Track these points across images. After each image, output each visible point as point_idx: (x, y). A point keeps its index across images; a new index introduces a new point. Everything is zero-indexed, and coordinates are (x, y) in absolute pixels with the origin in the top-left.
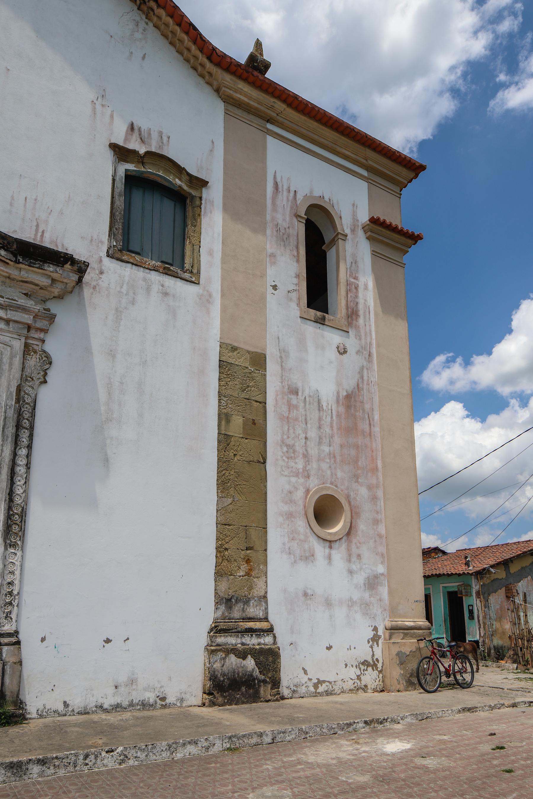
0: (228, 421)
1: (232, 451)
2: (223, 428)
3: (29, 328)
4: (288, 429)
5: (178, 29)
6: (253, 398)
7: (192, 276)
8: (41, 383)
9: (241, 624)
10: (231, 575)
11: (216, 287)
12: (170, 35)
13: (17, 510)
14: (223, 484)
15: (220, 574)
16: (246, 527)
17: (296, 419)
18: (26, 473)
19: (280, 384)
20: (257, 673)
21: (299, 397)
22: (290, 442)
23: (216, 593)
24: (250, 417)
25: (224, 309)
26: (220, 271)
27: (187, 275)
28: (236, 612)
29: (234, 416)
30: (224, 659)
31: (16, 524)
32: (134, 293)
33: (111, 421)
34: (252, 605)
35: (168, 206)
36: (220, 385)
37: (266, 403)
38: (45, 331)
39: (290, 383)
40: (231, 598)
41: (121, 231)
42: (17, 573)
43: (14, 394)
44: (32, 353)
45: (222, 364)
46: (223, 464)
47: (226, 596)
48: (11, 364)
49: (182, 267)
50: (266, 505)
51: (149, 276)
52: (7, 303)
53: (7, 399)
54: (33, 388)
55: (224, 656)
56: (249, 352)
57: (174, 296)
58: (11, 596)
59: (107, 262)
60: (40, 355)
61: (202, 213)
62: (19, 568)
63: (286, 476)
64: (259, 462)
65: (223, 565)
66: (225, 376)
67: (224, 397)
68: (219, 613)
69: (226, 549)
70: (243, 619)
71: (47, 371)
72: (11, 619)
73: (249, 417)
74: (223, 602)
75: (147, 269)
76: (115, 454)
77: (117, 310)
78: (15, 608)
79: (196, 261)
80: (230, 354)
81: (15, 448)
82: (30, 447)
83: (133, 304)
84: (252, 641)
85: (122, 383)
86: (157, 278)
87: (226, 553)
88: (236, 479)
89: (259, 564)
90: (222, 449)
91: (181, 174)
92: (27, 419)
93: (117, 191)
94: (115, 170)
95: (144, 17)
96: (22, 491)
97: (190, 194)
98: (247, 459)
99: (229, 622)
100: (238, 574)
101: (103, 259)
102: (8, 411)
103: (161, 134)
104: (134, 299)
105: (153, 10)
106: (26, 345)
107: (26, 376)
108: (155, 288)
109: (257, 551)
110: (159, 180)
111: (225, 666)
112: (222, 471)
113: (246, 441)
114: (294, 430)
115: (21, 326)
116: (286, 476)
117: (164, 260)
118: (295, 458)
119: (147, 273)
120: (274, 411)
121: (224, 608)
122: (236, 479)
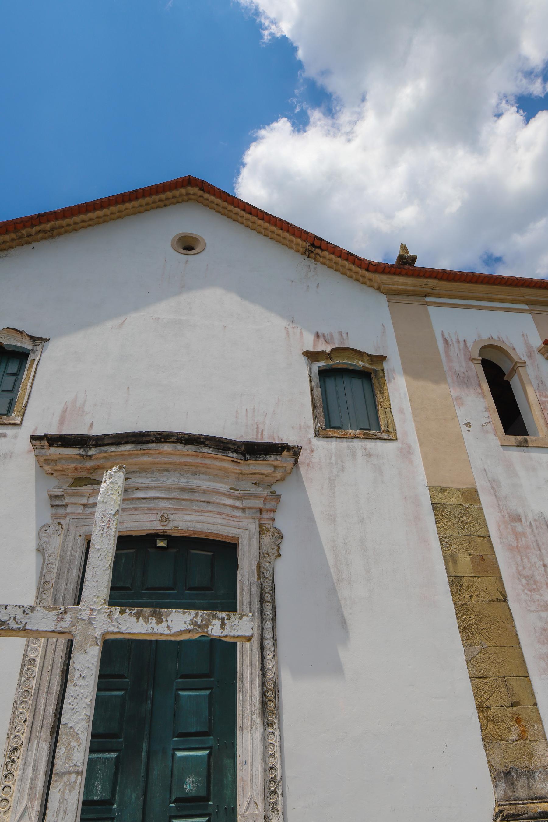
0: (455, 562)
1: (467, 593)
2: (451, 570)
3: (261, 511)
4: (521, 559)
5: (339, 259)
6: (475, 534)
7: (390, 435)
8: (276, 557)
9: (531, 806)
10: (502, 740)
11: (413, 438)
12: (334, 265)
13: (270, 686)
14: (466, 631)
16: (504, 677)
17: (527, 547)
18: (274, 645)
19: (499, 514)
21: (523, 523)
22: (527, 572)
23: (490, 766)
24: (477, 554)
25: (425, 457)
26: (413, 424)
27: (384, 435)
28: (520, 790)
29: (459, 556)
31: (270, 700)
32: (342, 461)
33: (342, 581)
34: (538, 778)
35: (357, 384)
36: (438, 528)
37: (489, 536)
38: (273, 511)
39: (509, 510)
40: (510, 771)
41: (322, 414)
42: (278, 755)
43: (256, 571)
44: (266, 532)
45: (435, 506)
46: (462, 610)
47: (503, 769)
48: (250, 545)
49: (379, 429)
50: (521, 649)
51: (352, 444)
52: (241, 494)
53: (250, 577)
54: (270, 563)
56: (458, 490)
57: (377, 455)
58: (275, 783)
59: (315, 441)
60: (273, 532)
61: (387, 381)
62: (279, 749)
63: (534, 611)
64: (499, 600)
65: (490, 728)
66: (441, 517)
67: (446, 538)
68: (501, 792)
69: (489, 708)
70: (532, 799)
71: (280, 546)
72: (278, 811)
73: (476, 553)
74: (502, 777)
75: (350, 438)
76: (351, 614)
77: (330, 479)
78: (280, 797)
79: (390, 422)
80: (441, 495)
81: (262, 623)
82: (274, 619)
83: (343, 471)
85: (345, 544)
86: (359, 443)
87: (490, 712)
88: (479, 623)
89: (532, 724)
90: (456, 593)
91: (362, 357)
92: (269, 593)
93: (314, 385)
94: (310, 370)
95: (313, 261)
96: (272, 665)
97: (373, 370)
98: (486, 599)
99: (515, 804)
101: (312, 440)
102: (252, 588)
103: (340, 334)
104: (343, 466)
105: (318, 254)
106: (261, 526)
107: (263, 553)
108: (359, 453)
109: (525, 706)
110: (345, 367)
112: (462, 616)
113: (479, 579)
114: (528, 558)
115: (254, 511)
116: (534, 611)
117: (362, 427)
118: (539, 590)
119: (350, 442)
120: (501, 543)
121: (504, 785)
122: (479, 623)
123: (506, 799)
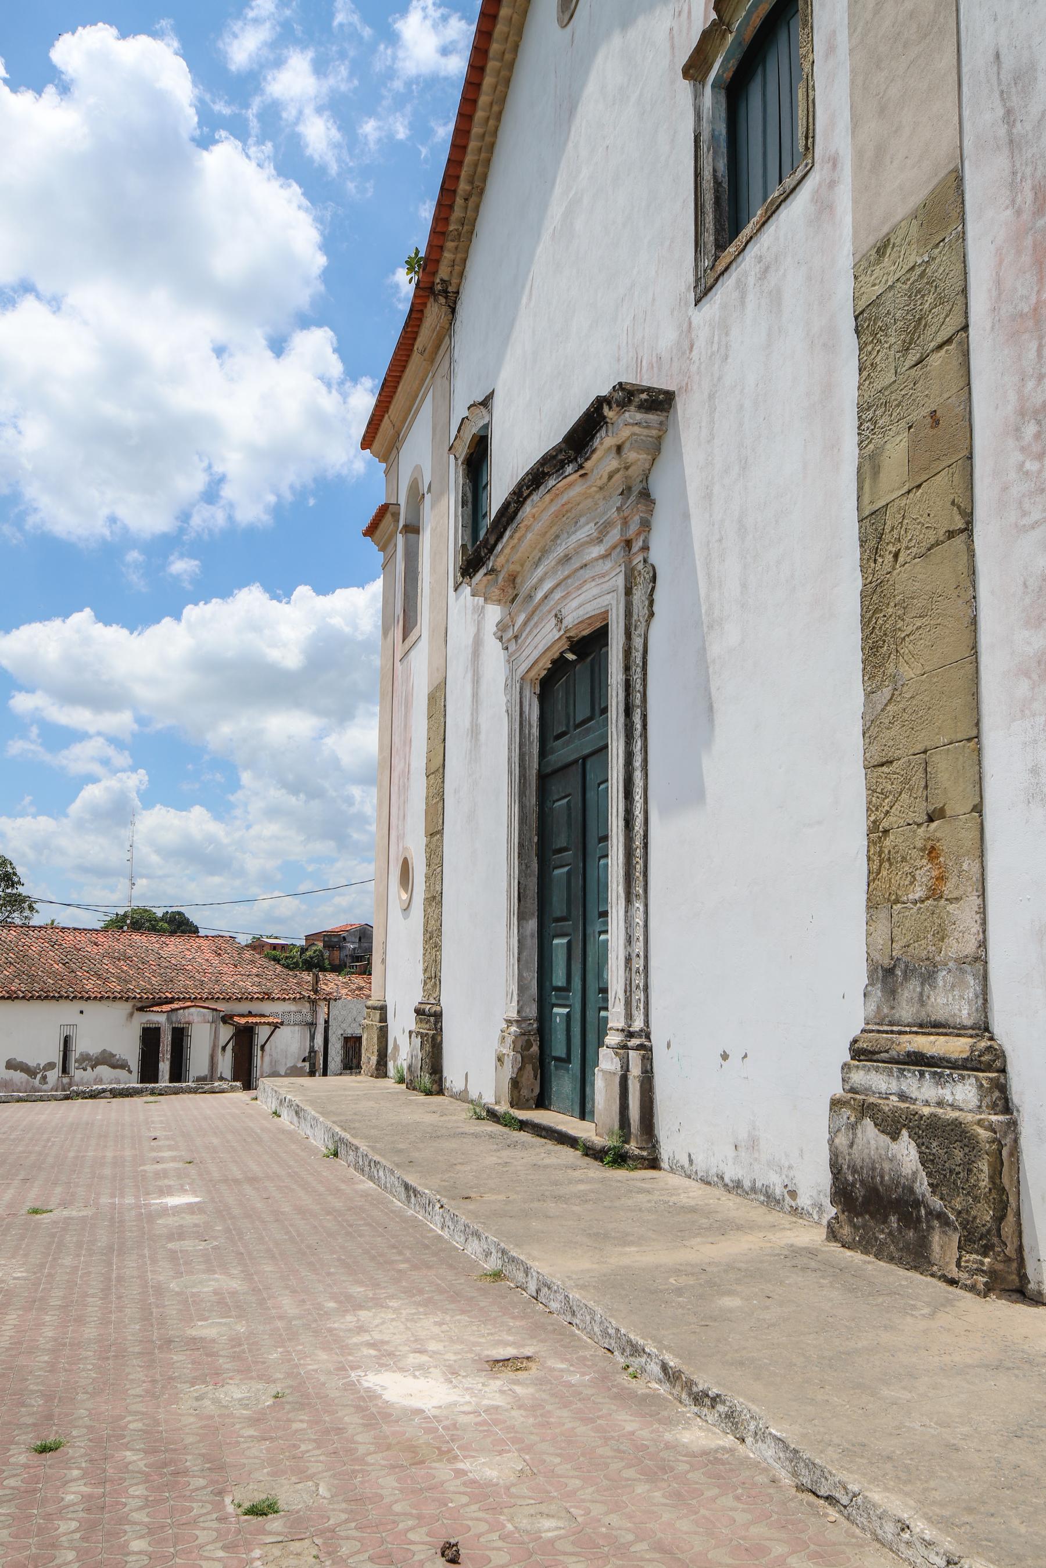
15: (880, 900)
20: (922, 1186)
30: (853, 1127)
40: (895, 966)
55: (853, 1119)
70: (921, 1026)
74: (878, 978)
84: (925, 1093)
100: (911, 897)
111: (855, 1147)
123: (878, 1021)
